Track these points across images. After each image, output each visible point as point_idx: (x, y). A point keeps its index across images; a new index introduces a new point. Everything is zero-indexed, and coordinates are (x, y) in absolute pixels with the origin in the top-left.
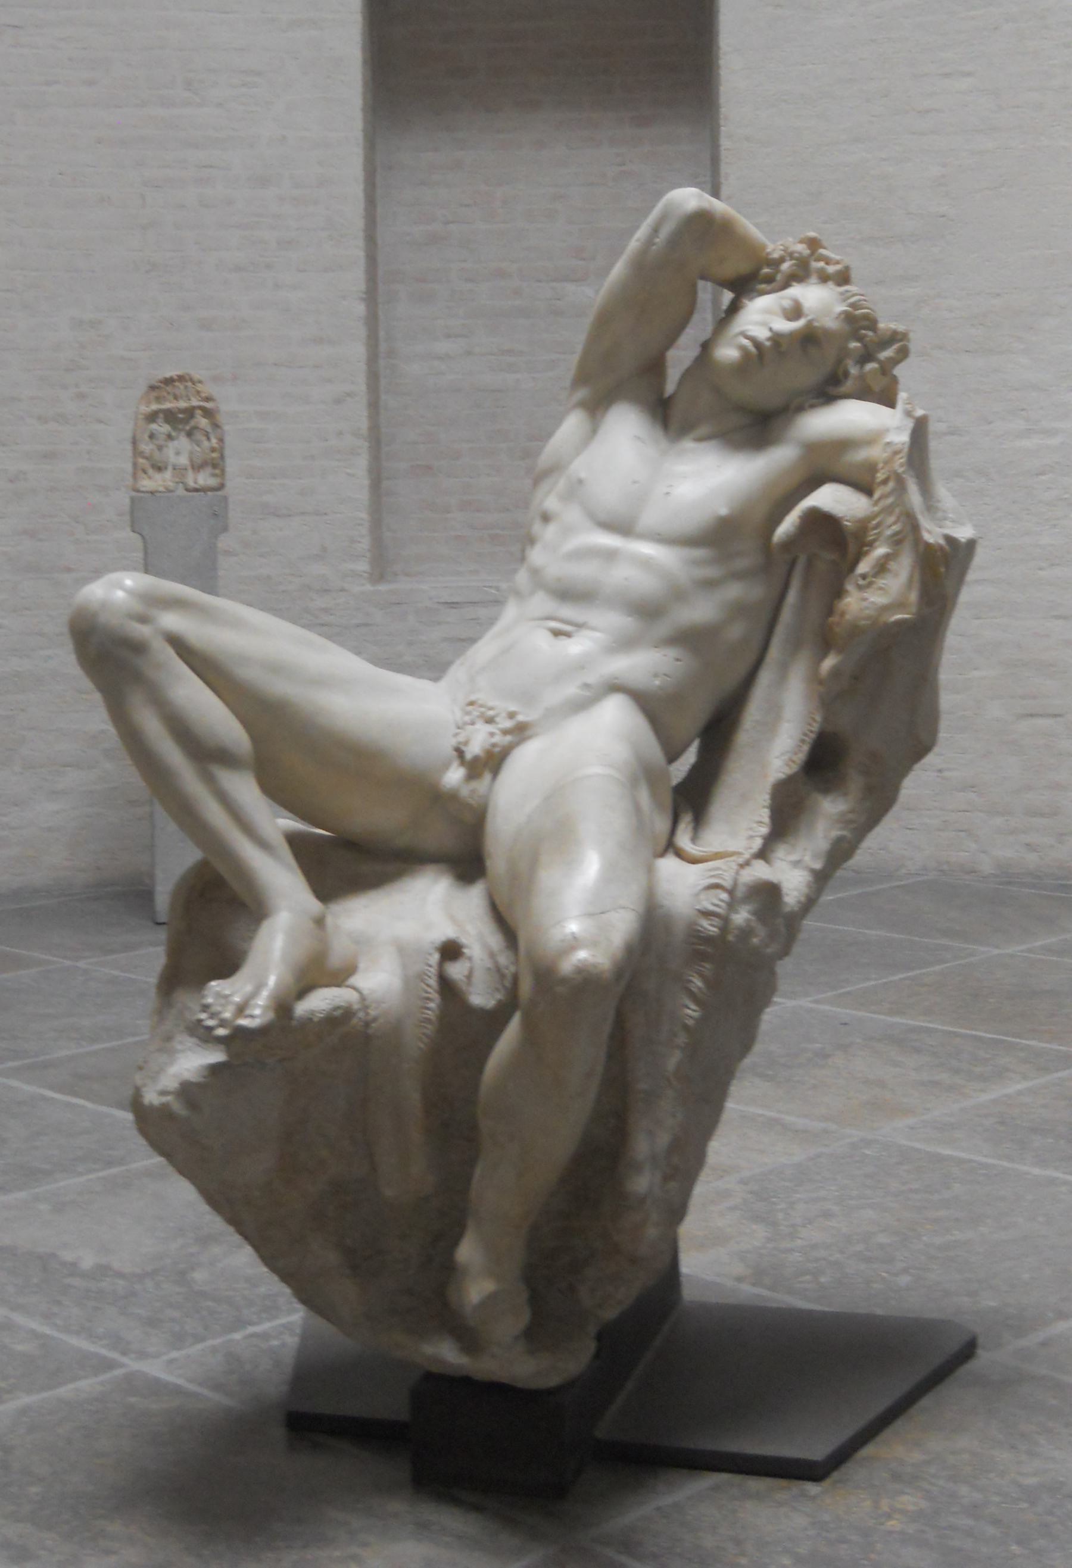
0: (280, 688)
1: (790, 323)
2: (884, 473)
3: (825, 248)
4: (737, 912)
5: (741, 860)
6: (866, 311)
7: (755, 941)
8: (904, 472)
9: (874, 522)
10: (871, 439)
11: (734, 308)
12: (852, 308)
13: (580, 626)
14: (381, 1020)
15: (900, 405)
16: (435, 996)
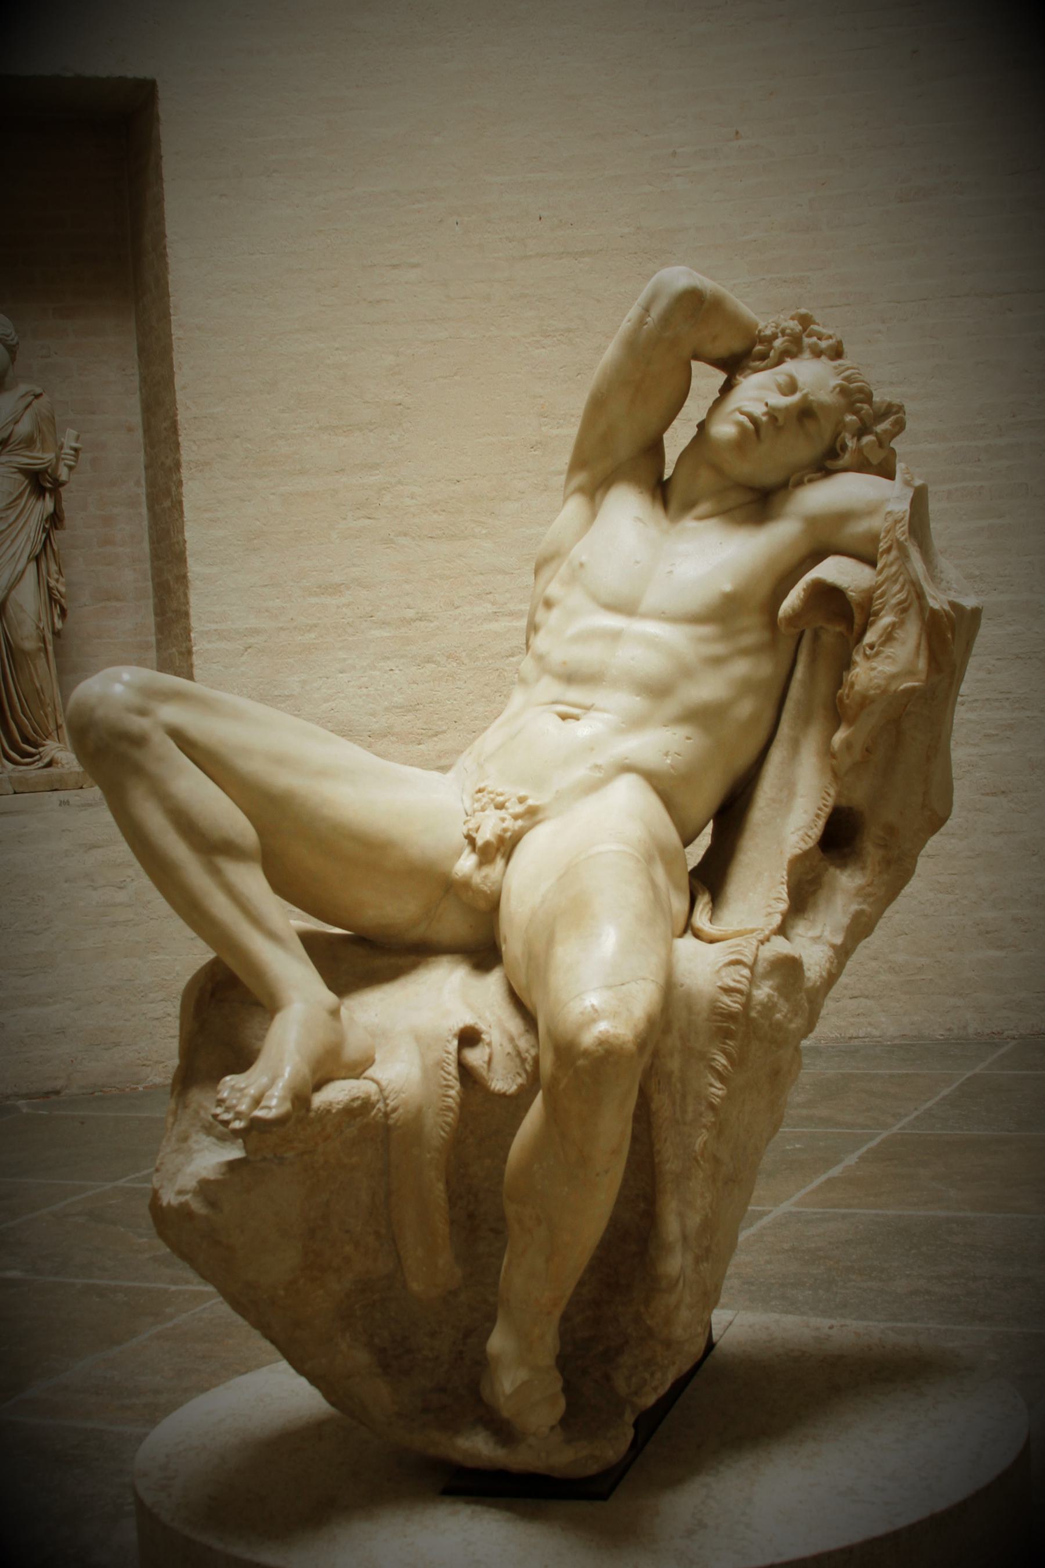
0: (284, 780)
1: (786, 398)
2: (886, 542)
3: (818, 324)
4: (759, 988)
5: (761, 937)
6: (859, 384)
7: (778, 1016)
8: (906, 540)
9: (879, 591)
10: (870, 511)
11: (727, 388)
12: (847, 382)
13: (588, 708)
14: (401, 1110)
15: (898, 476)
16: (457, 1085)
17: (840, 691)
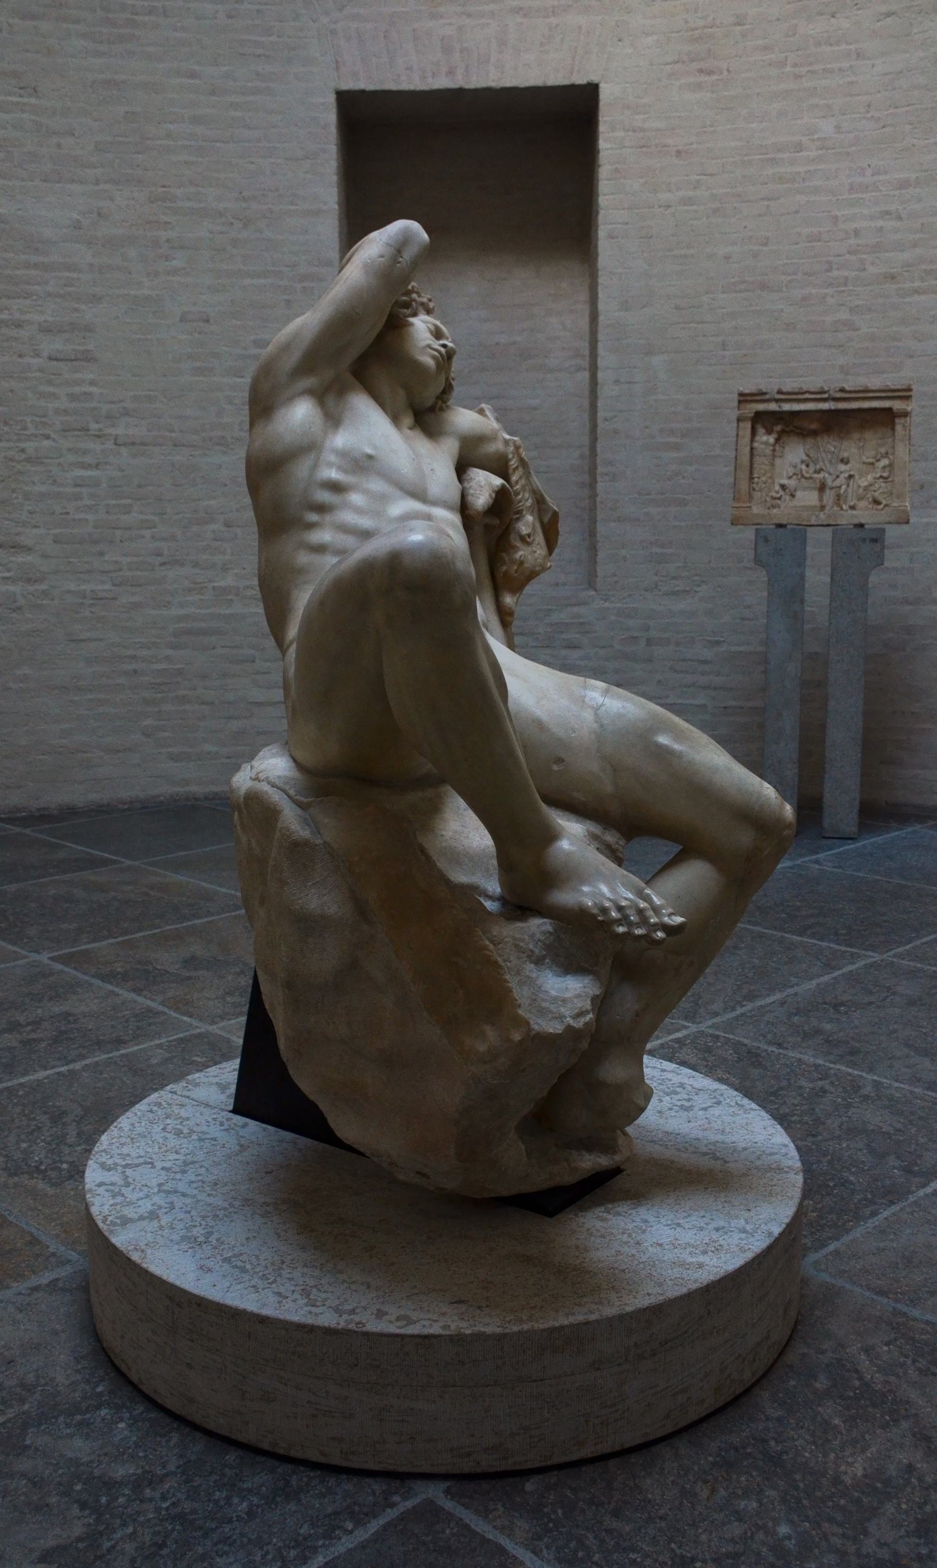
9: (520, 497)
17: (505, 568)
